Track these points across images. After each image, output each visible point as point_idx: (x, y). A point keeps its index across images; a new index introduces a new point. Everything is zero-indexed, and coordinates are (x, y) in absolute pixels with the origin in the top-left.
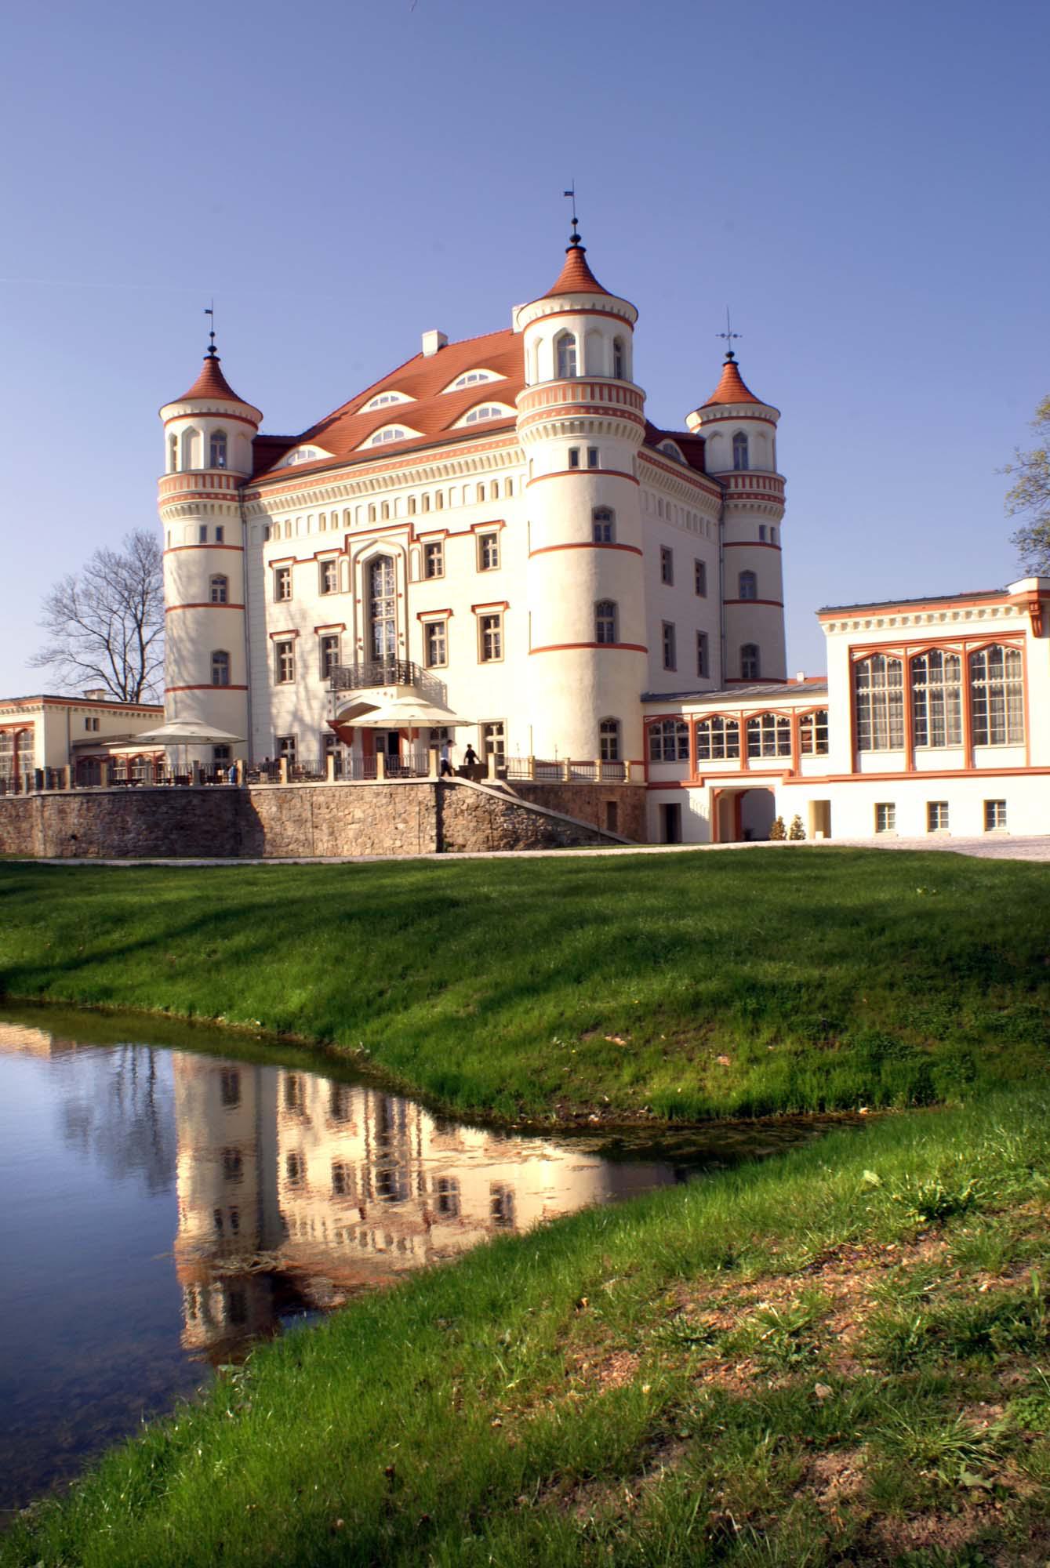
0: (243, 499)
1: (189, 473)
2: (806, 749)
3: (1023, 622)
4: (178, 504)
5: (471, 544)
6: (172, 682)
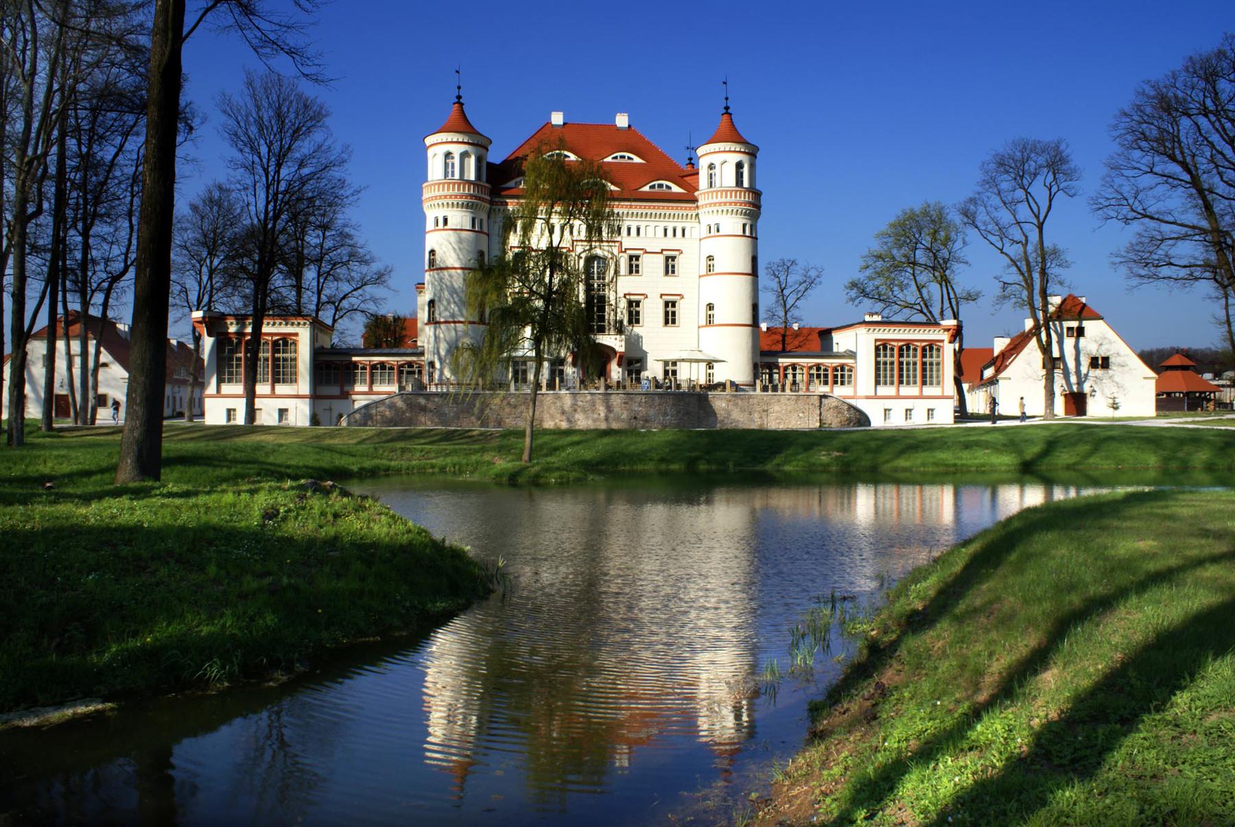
0: (491, 203)
1: (463, 180)
2: (836, 382)
3: (946, 337)
4: (460, 201)
5: (660, 259)
6: (453, 315)
